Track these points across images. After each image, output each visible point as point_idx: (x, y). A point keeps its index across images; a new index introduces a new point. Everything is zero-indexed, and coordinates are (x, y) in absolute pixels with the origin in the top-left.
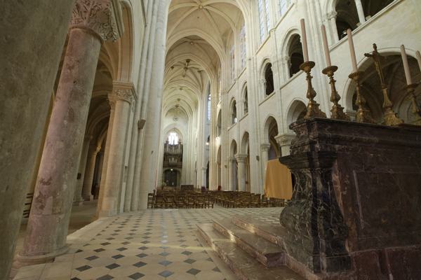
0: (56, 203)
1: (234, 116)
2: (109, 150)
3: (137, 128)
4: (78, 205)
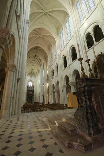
1: (53, 75)
2: (5, 91)
3: (17, 81)
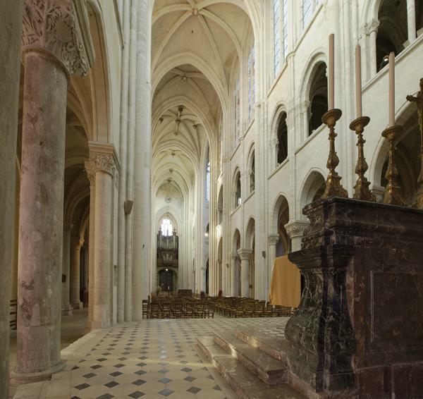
0: (43, 312)
1: (238, 195)
2: (93, 243)
3: (123, 214)
4: (67, 315)
